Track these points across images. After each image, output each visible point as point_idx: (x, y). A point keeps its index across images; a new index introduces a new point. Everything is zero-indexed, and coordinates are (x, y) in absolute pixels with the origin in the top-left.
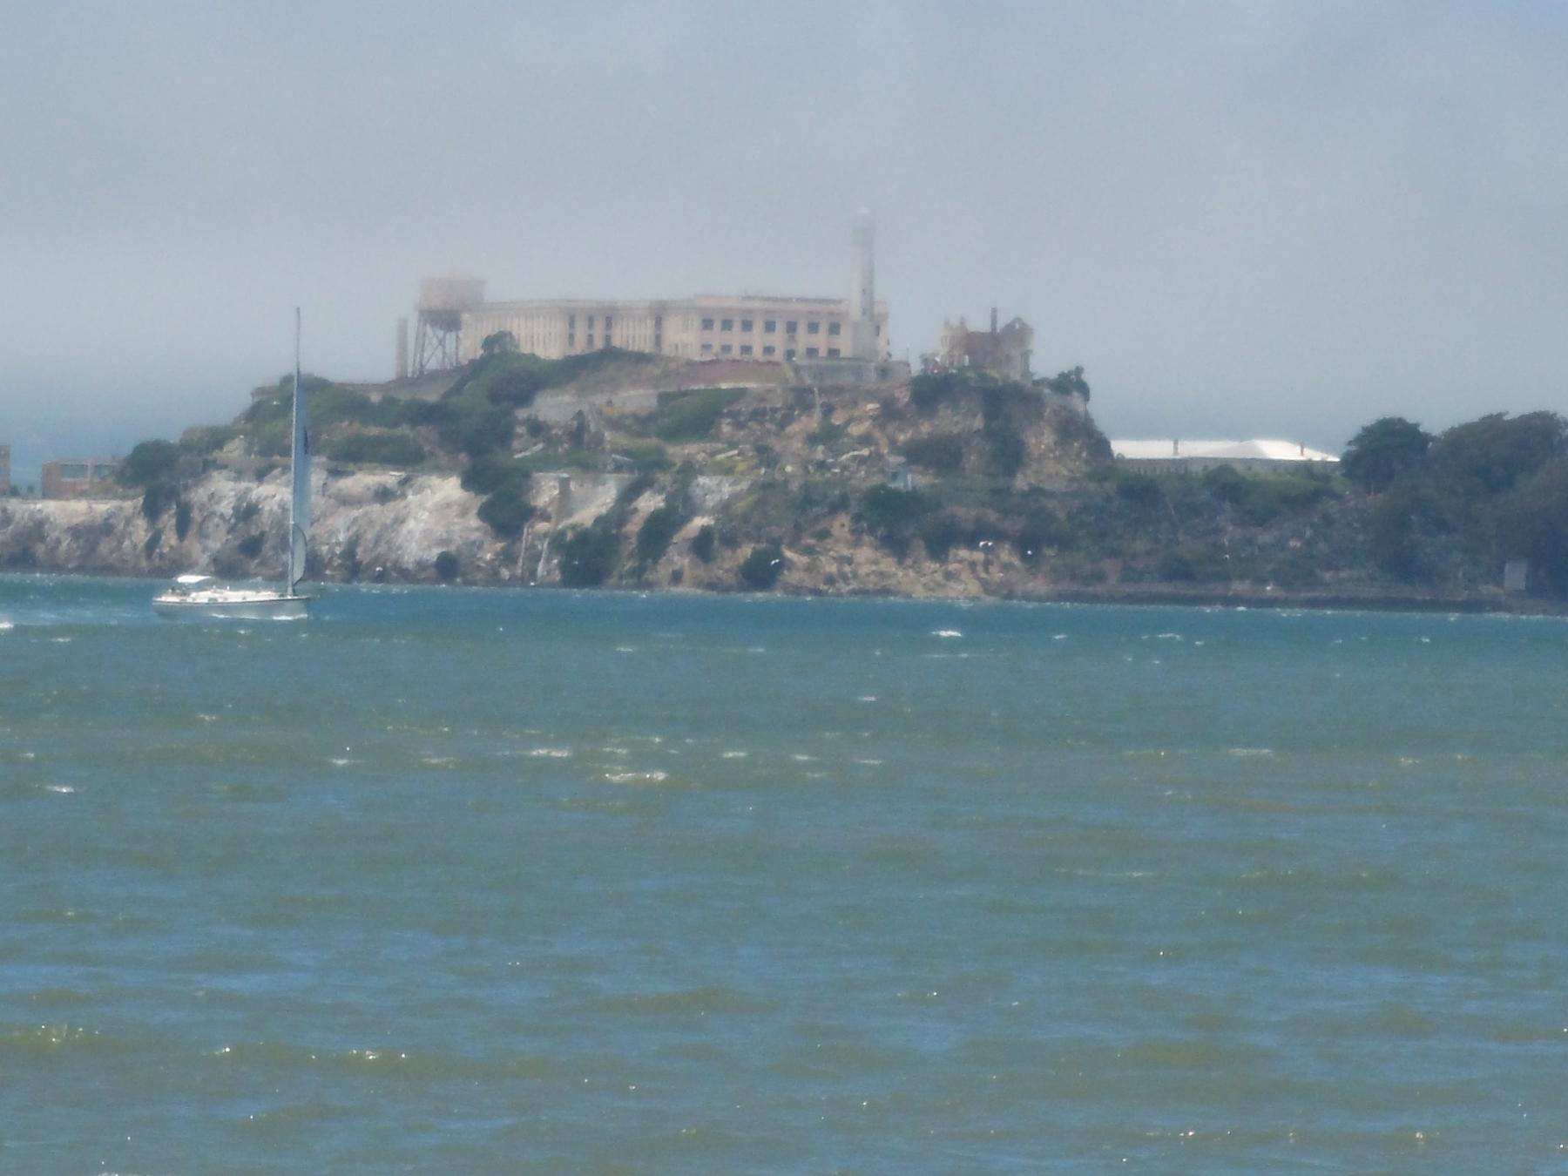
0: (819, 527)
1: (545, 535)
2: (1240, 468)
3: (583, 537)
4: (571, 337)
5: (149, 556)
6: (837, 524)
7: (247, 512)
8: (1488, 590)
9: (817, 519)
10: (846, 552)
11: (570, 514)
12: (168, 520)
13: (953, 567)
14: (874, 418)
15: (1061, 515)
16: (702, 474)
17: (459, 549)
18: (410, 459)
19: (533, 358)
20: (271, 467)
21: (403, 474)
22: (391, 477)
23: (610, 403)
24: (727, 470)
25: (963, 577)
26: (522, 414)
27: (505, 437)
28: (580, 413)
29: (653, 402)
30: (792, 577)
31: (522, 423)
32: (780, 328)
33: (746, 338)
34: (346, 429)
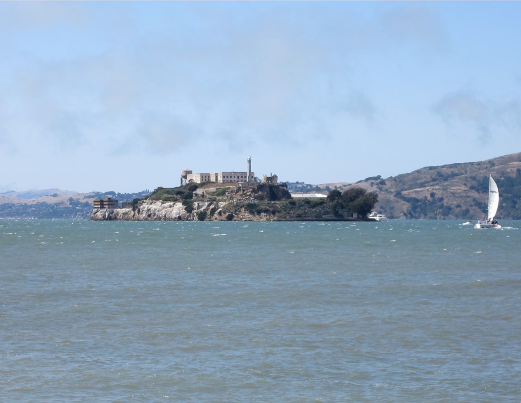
0: (239, 210)
1: (196, 212)
2: (309, 199)
3: (201, 213)
4: (202, 180)
5: (133, 218)
6: (242, 209)
7: (149, 210)
8: (350, 218)
9: (239, 209)
10: (243, 214)
11: (199, 209)
12: (136, 211)
13: (261, 216)
14: (251, 192)
15: (279, 207)
16: (220, 201)
17: (181, 215)
18: (175, 200)
19: (196, 183)
20: (153, 202)
21: (173, 203)
22: (172, 203)
23: (208, 190)
24: (225, 201)
25: (263, 218)
26: (194, 192)
27: (191, 197)
28: (203, 192)
29: (215, 190)
30: (235, 218)
31: (194, 194)
32: (236, 177)
33: (231, 179)
34: (165, 195)
